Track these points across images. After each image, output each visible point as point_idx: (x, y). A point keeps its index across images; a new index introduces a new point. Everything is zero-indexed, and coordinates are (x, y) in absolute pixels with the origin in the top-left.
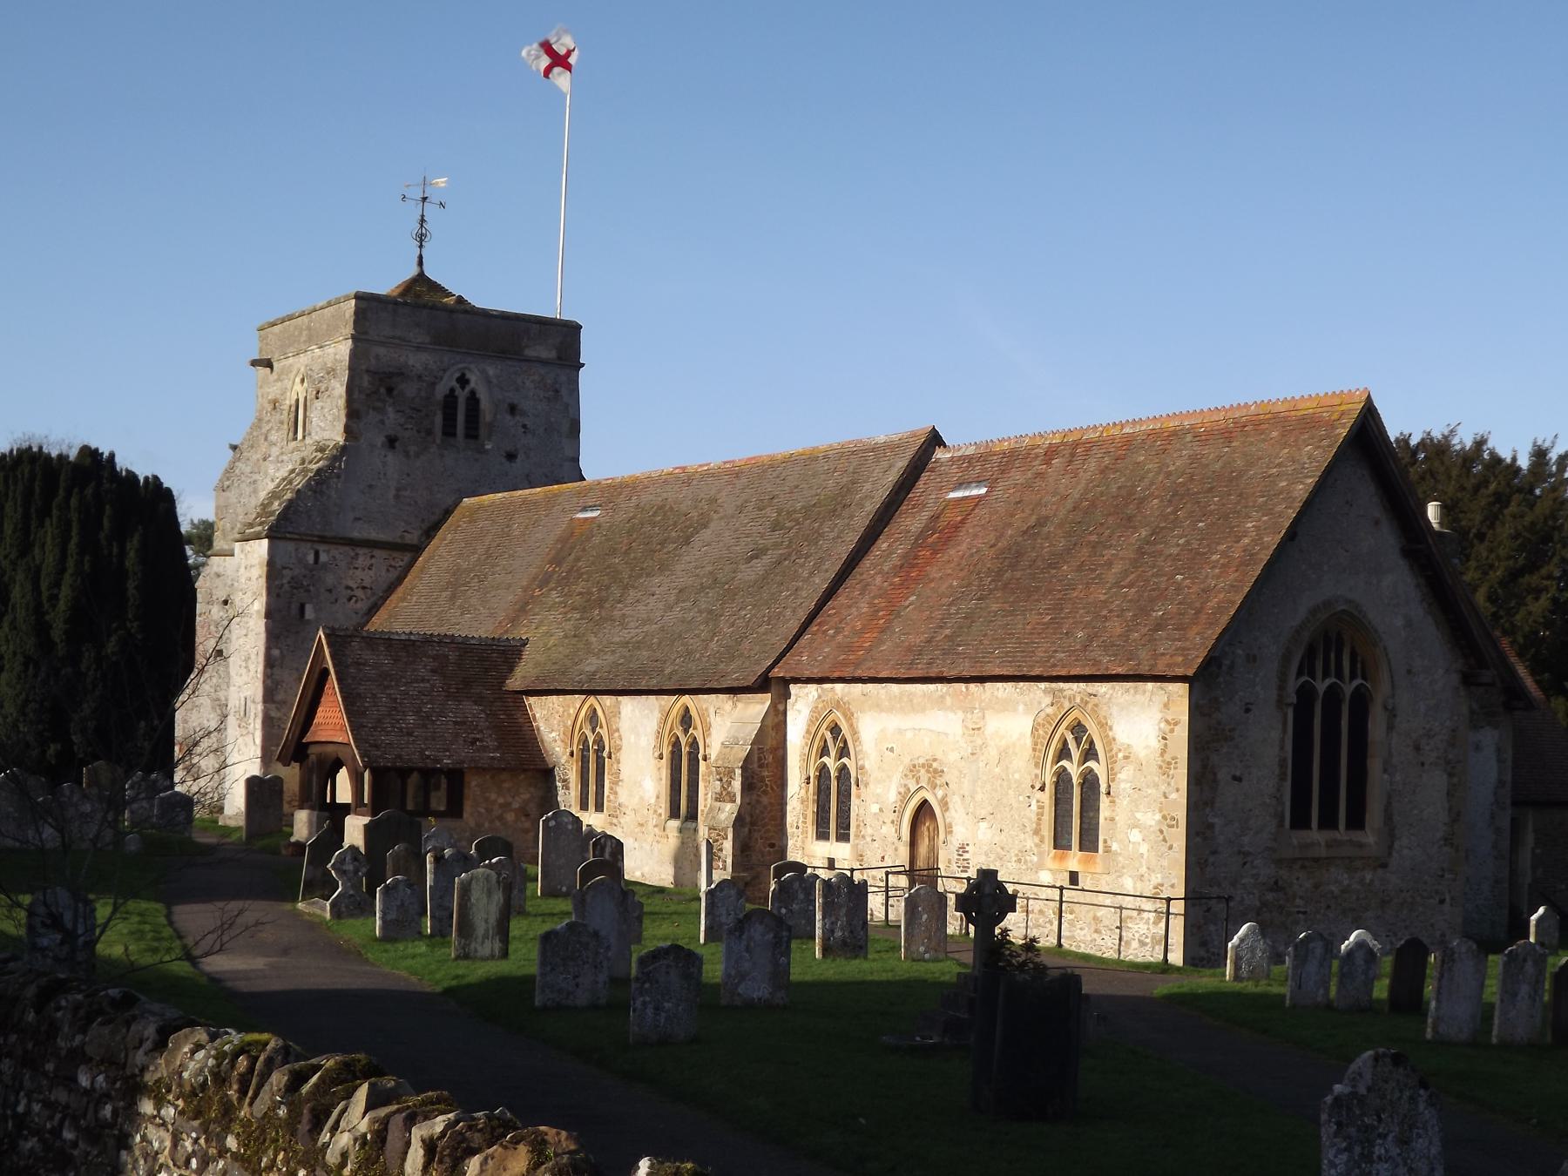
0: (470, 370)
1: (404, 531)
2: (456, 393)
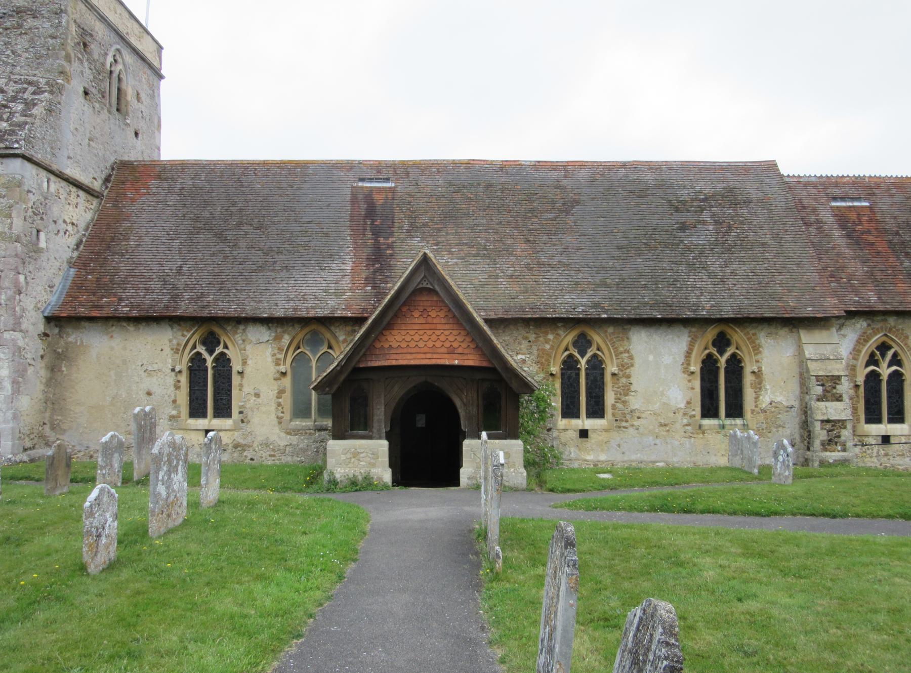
1: (94, 178)
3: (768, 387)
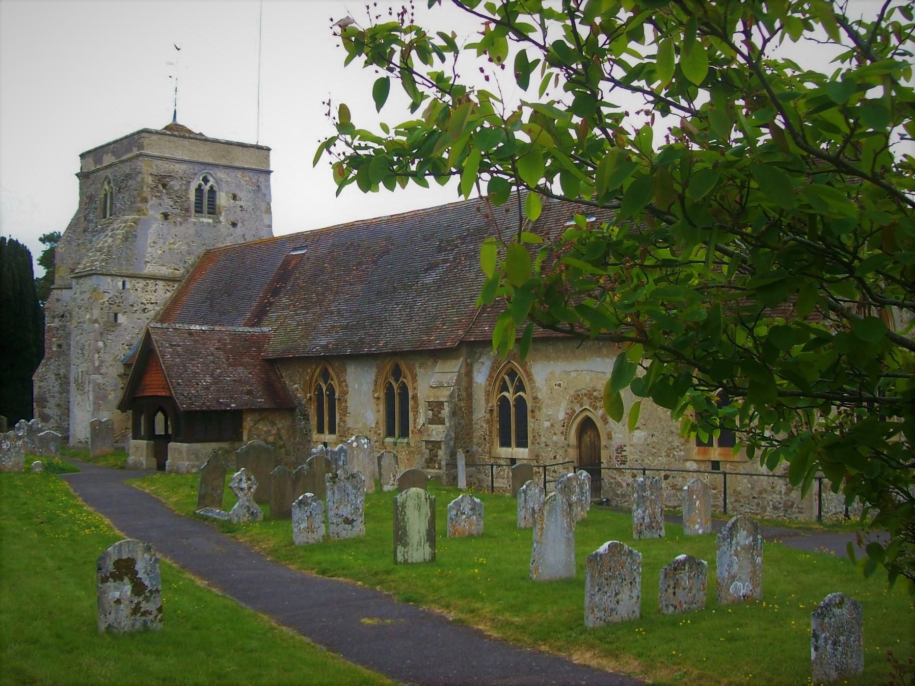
0: (210, 174)
2: (202, 188)
3: (421, 411)
